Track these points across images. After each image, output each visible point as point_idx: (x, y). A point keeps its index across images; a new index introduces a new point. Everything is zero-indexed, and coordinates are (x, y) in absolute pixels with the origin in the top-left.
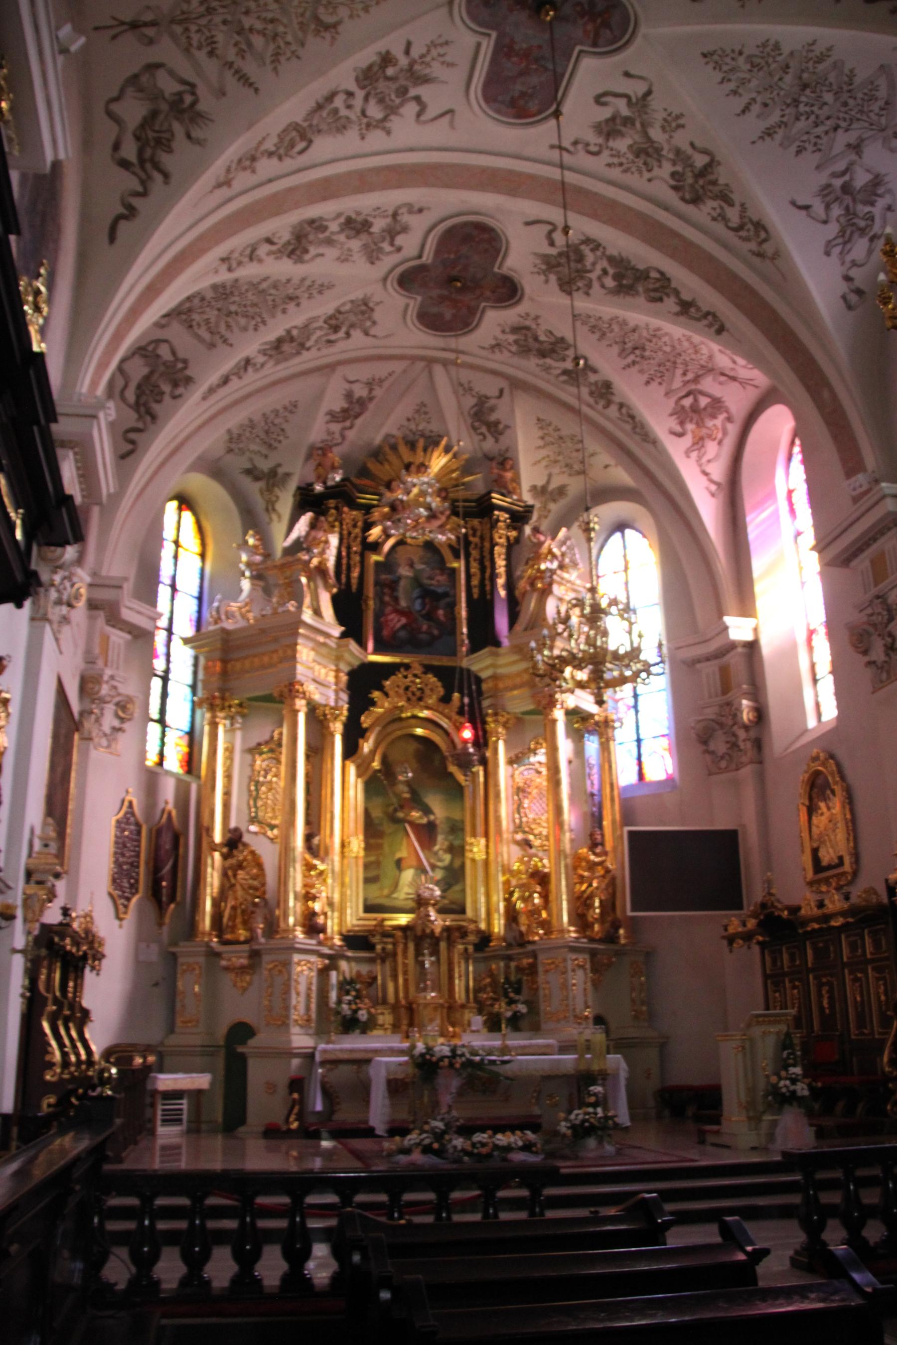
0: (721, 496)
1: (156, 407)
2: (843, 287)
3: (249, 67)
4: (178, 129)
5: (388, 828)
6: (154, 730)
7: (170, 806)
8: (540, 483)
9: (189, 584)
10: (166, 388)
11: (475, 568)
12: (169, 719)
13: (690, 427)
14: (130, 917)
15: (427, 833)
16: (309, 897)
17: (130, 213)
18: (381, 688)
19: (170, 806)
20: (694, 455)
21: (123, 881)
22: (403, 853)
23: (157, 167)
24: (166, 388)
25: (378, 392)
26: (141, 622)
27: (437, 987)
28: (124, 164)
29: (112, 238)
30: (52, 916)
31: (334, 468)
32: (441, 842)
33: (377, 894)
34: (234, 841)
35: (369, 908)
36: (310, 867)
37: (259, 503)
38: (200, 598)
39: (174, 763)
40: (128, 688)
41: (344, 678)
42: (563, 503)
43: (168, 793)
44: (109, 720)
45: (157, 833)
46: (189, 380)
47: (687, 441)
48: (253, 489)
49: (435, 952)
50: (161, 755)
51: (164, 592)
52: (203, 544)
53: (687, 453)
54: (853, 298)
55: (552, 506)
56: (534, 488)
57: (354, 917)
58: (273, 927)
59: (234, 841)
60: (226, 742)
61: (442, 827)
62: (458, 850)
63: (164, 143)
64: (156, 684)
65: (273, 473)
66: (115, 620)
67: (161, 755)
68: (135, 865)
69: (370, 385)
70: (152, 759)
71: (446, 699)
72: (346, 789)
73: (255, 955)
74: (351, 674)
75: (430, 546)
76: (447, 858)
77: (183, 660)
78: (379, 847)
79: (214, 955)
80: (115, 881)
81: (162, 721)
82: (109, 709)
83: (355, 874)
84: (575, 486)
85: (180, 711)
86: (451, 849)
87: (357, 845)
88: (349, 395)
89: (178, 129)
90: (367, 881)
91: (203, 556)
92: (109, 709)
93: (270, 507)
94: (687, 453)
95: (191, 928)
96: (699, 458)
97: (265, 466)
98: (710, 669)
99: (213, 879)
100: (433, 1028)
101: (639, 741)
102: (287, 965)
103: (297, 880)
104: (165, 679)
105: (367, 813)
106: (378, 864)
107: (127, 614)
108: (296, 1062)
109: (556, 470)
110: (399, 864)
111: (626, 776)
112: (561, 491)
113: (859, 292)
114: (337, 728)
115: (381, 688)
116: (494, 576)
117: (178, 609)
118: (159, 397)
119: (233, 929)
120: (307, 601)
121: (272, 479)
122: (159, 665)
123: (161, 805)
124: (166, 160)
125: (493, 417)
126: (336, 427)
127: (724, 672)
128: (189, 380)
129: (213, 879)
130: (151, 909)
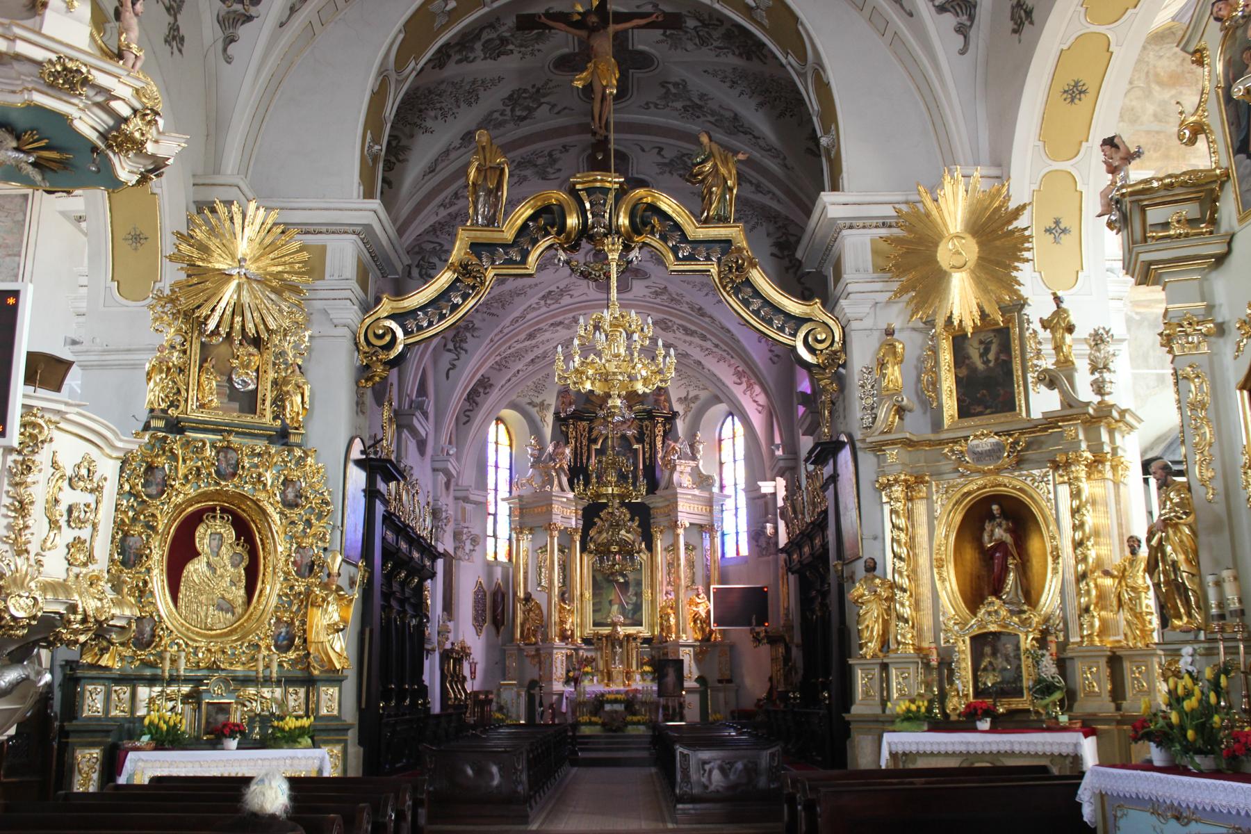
0: (765, 412)
1: (478, 399)
2: (770, 355)
3: (493, 311)
4: (468, 335)
5: (605, 585)
6: (490, 541)
8: (683, 395)
9: (504, 462)
10: (481, 390)
11: (647, 447)
13: (744, 380)
14: (483, 635)
15: (625, 587)
16: (562, 622)
17: (454, 366)
18: (599, 517)
21: (479, 621)
22: (612, 597)
24: (481, 390)
26: (480, 499)
27: (622, 662)
28: (449, 351)
29: (448, 377)
30: (448, 646)
31: (570, 404)
32: (631, 590)
33: (599, 619)
34: (528, 598)
35: (595, 624)
36: (562, 610)
37: (538, 418)
38: (511, 469)
39: (503, 558)
41: (580, 512)
42: (698, 403)
43: (498, 573)
44: (468, 547)
45: (495, 594)
46: (491, 385)
47: (744, 386)
49: (621, 647)
50: (496, 553)
51: (491, 470)
52: (511, 439)
54: (776, 359)
56: (680, 400)
57: (589, 630)
58: (546, 638)
59: (528, 598)
60: (525, 543)
61: (632, 583)
62: (639, 595)
63: (464, 340)
64: (491, 518)
65: (542, 404)
66: (466, 500)
67: (496, 553)
68: (484, 611)
70: (490, 557)
71: (632, 519)
72: (583, 566)
73: (538, 650)
74: (584, 509)
75: (624, 437)
76: (634, 599)
77: (504, 509)
78: (601, 594)
79: (520, 650)
80: (475, 619)
81: (495, 536)
82: (468, 542)
83: (589, 608)
84: (704, 395)
85: (504, 529)
86: (636, 594)
87: (588, 594)
89: (468, 335)
90: (594, 611)
91: (511, 446)
92: (468, 542)
93: (543, 420)
95: (512, 638)
97: (538, 401)
98: (761, 502)
99: (520, 617)
100: (619, 681)
101: (737, 533)
102: (551, 654)
103: (555, 617)
104: (495, 515)
105: (594, 577)
106: (600, 603)
107: (472, 497)
108: (555, 697)
109: (690, 389)
110: (611, 602)
111: (730, 553)
112: (696, 398)
113: (777, 356)
114: (577, 538)
115: (599, 517)
116: (656, 453)
117: (499, 480)
118: (478, 395)
119: (529, 638)
120: (556, 482)
121: (542, 406)
122: (492, 510)
124: (465, 346)
127: (766, 504)
128: (491, 385)
129: (520, 617)
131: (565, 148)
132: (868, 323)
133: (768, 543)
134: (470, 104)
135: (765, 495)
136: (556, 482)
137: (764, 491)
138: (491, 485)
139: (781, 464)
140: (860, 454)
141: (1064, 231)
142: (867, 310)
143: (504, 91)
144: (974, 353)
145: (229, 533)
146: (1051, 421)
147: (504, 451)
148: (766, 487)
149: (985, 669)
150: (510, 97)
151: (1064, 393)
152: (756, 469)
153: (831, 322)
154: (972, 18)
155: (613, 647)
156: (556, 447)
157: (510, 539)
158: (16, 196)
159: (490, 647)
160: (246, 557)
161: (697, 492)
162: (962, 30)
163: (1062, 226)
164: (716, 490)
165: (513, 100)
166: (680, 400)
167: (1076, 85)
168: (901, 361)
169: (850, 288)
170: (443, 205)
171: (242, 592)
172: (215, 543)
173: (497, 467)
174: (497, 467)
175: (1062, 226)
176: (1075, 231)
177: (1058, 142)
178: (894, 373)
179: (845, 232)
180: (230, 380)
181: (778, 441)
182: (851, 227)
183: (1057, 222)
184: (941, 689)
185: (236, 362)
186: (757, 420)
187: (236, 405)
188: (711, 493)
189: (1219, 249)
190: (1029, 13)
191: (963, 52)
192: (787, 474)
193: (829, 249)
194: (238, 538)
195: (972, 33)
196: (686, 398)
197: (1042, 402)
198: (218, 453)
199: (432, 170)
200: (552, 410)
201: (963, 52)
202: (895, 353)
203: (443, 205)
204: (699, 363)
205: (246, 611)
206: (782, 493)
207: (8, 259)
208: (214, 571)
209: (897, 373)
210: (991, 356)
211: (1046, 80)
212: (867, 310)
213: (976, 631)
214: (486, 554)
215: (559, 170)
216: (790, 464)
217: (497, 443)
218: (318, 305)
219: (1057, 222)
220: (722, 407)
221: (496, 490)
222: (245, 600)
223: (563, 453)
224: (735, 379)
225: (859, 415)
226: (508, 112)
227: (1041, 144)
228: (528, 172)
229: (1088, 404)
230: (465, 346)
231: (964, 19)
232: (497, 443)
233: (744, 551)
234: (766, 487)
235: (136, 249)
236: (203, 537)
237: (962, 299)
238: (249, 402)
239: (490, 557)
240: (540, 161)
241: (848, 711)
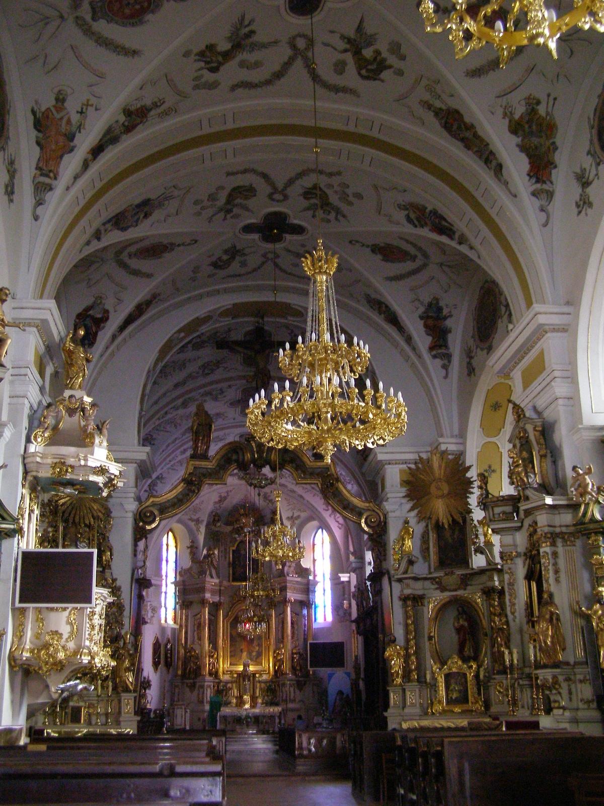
0: (343, 529)
6: (163, 610)
7: (170, 637)
8: (290, 516)
9: (172, 558)
12: (167, 606)
19: (170, 637)
20: (333, 516)
21: (156, 664)
23: (154, 490)
25: (230, 493)
32: (255, 643)
37: (194, 528)
40: (155, 604)
48: (192, 524)
49: (249, 680)
51: (164, 563)
52: (176, 542)
53: (330, 516)
55: (296, 522)
56: (288, 518)
69: (227, 492)
76: (257, 648)
82: (150, 611)
84: (304, 515)
88: (220, 496)
91: (176, 547)
93: (198, 530)
94: (330, 516)
96: (335, 516)
97: (195, 518)
104: (166, 593)
109: (295, 511)
110: (242, 651)
112: (299, 517)
120: (208, 573)
121: (198, 521)
123: (166, 636)
124: (156, 488)
125: (270, 498)
126: (217, 505)
130: (164, 669)
131: (230, 386)
132: (397, 514)
133: (345, 614)
134: (181, 370)
135: (343, 582)
136: (208, 573)
137: (343, 579)
138: (164, 573)
139: (354, 565)
140: (394, 584)
141: (494, 471)
142: (397, 507)
143: (200, 363)
144: (448, 534)
146: (482, 571)
147: (172, 549)
148: (344, 577)
149: (452, 690)
150: (203, 366)
151: (487, 557)
152: (339, 563)
153: (378, 511)
154: (450, 362)
155: (244, 680)
156: (208, 550)
157: (175, 609)
159: (162, 681)
161: (299, 579)
162: (445, 367)
163: (492, 469)
164: (311, 578)
165: (204, 367)
166: (288, 518)
167: (497, 403)
168: (412, 537)
169: (389, 495)
170: (159, 419)
173: (167, 561)
174: (167, 561)
175: (492, 469)
176: (498, 470)
177: (490, 428)
178: (409, 543)
179: (386, 466)
181: (351, 549)
182: (389, 464)
183: (490, 467)
184: (431, 701)
186: (338, 533)
188: (309, 580)
189: (519, 524)
190: (474, 370)
191: (446, 377)
192: (358, 571)
193: (378, 473)
195: (450, 369)
196: (292, 517)
197: (478, 561)
199: (156, 403)
200: (205, 523)
201: (446, 377)
202: (409, 534)
203: (159, 419)
204: (301, 497)
206: (354, 582)
209: (410, 543)
210: (455, 536)
211: (482, 402)
212: (397, 507)
213: (447, 671)
214: (160, 620)
215: (225, 397)
216: (358, 565)
217: (167, 545)
218: (118, 500)
219: (490, 467)
220: (315, 523)
221: (166, 576)
223: (214, 554)
224: (324, 507)
225: (392, 562)
226: (201, 372)
227: (481, 430)
228: (207, 398)
229: (497, 564)
230: (156, 488)
231: (446, 362)
232: (167, 545)
233: (330, 618)
234: (344, 577)
237: (440, 508)
239: (163, 621)
240: (214, 393)
241: (386, 711)
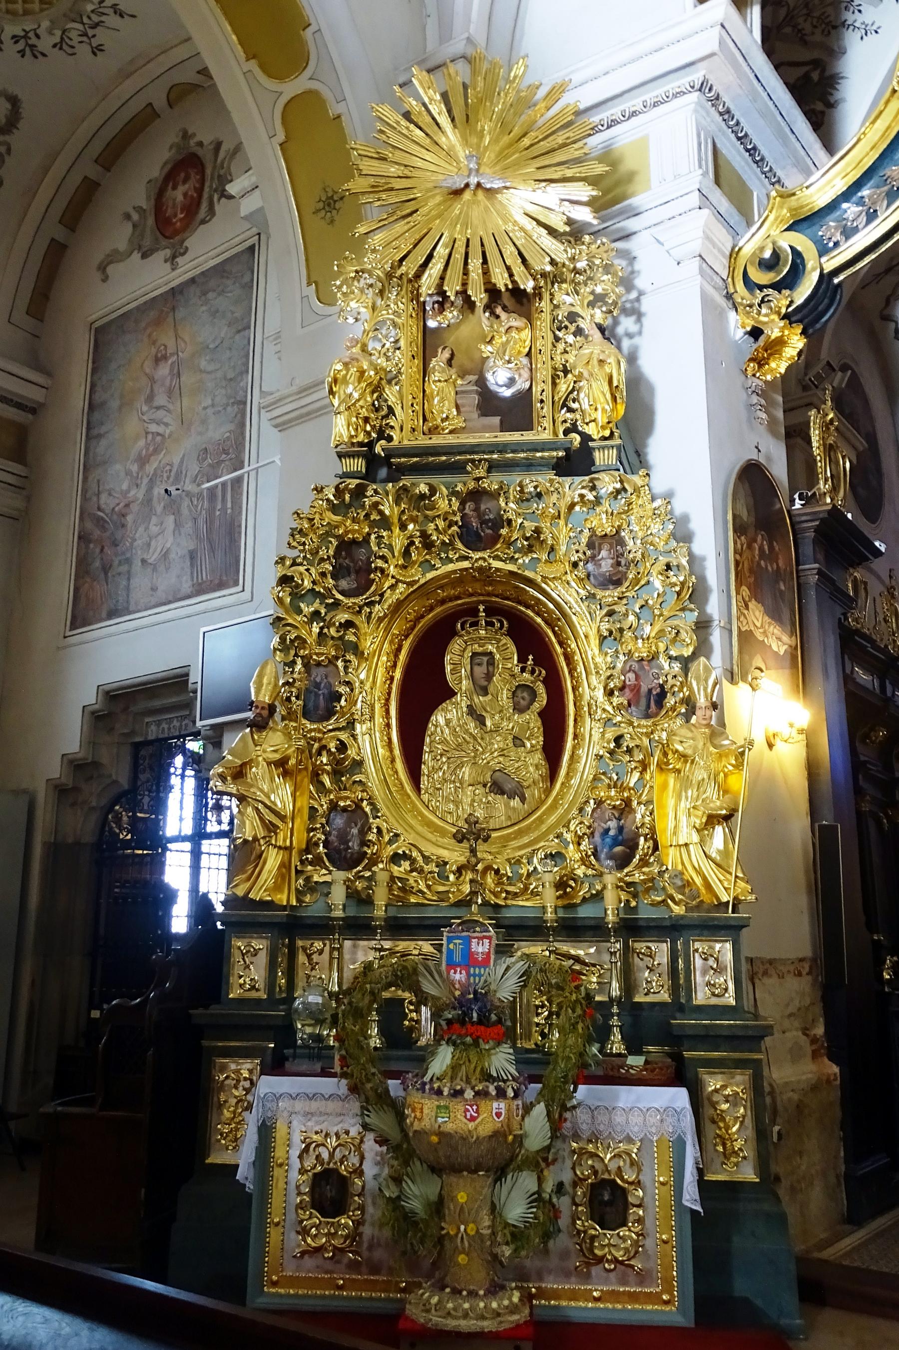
145: (505, 652)
158: (243, 252)
160: (541, 689)
171: (538, 757)
172: (480, 671)
180: (481, 382)
185: (487, 349)
187: (496, 420)
194: (522, 659)
198: (463, 503)
205: (548, 792)
207: (237, 337)
208: (481, 720)
222: (544, 771)
235: (332, 222)
236: (456, 660)
238: (517, 412)
